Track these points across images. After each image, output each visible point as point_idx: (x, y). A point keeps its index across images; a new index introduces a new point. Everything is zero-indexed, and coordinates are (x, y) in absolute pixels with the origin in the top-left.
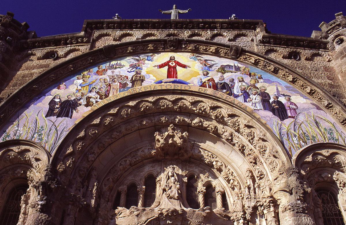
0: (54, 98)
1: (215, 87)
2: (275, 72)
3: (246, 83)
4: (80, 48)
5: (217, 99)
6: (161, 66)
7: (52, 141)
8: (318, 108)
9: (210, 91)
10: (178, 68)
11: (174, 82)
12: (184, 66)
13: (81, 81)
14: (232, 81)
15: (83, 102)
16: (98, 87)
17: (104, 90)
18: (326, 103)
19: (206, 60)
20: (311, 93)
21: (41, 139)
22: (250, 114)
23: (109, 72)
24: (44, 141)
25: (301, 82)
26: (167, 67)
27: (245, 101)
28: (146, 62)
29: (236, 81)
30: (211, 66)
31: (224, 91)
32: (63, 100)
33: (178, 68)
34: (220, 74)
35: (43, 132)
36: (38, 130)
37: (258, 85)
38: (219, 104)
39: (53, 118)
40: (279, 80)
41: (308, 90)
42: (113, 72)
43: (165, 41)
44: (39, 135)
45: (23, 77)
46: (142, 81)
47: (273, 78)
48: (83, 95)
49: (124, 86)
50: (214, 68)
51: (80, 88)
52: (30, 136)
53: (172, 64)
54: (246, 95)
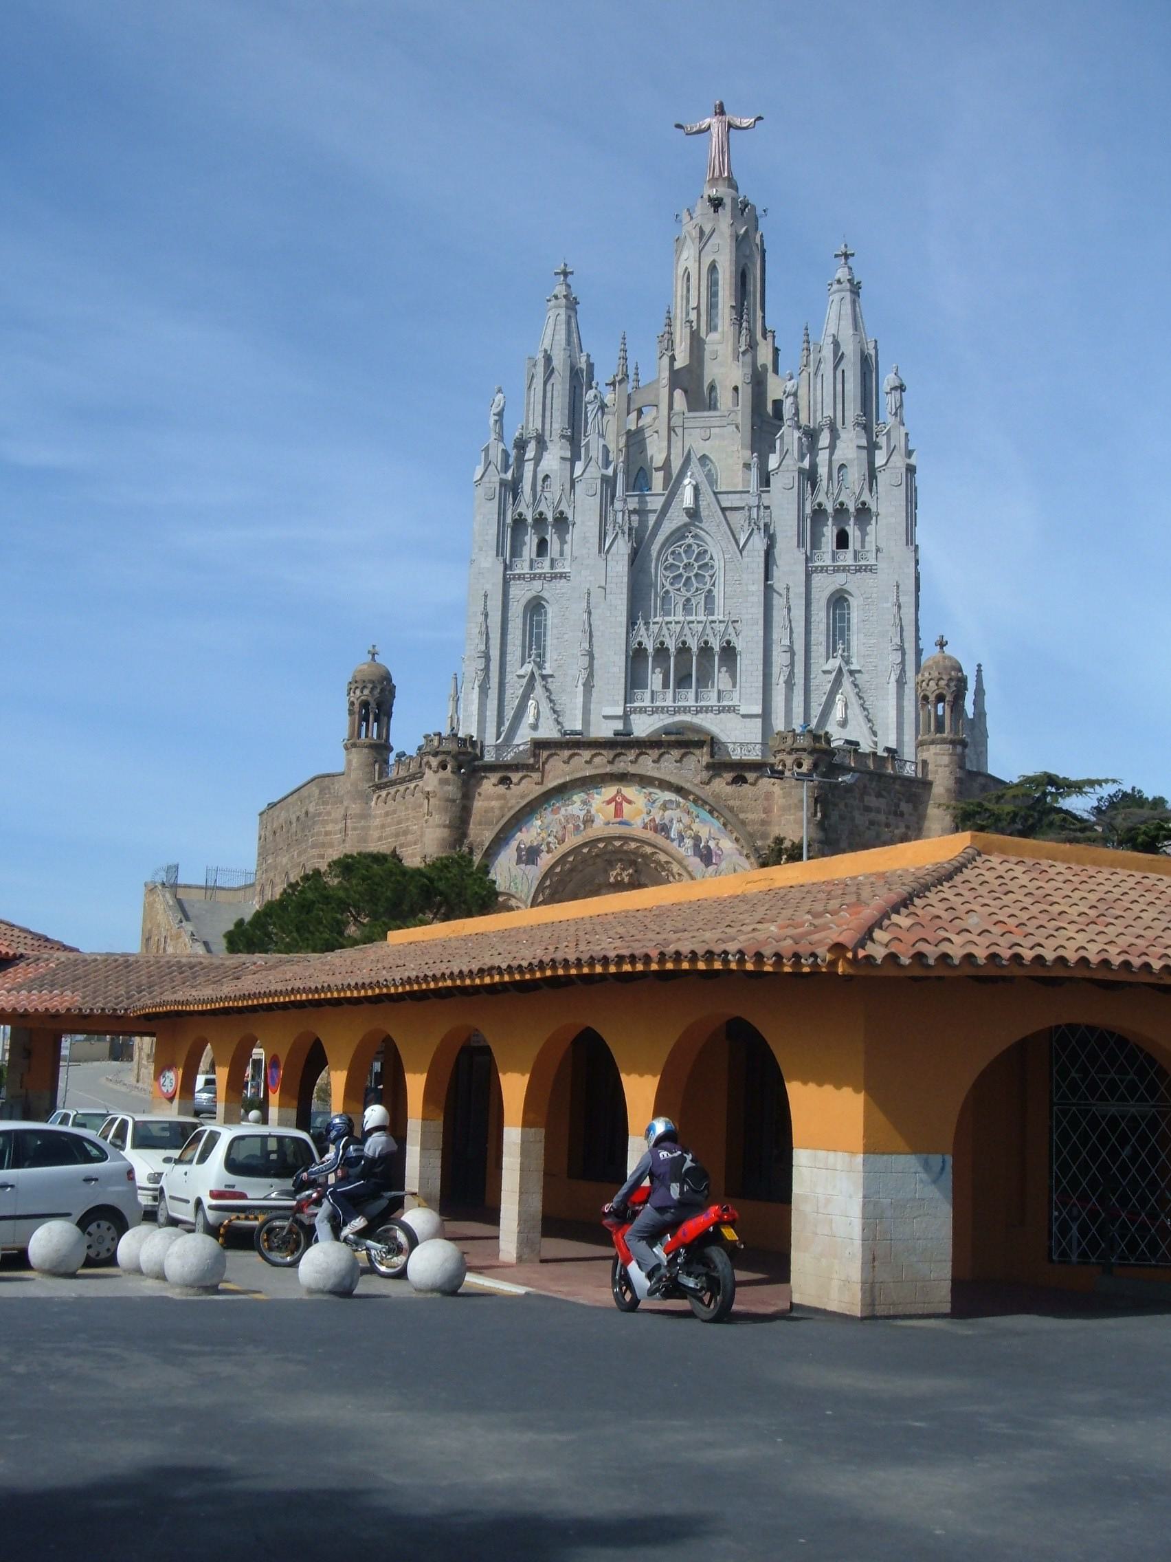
0: (519, 844)
1: (656, 831)
2: (711, 812)
3: (684, 824)
4: (532, 774)
5: (655, 846)
6: (609, 802)
7: (526, 890)
8: (741, 854)
9: (649, 835)
10: (625, 804)
11: (621, 823)
12: (630, 802)
13: (538, 823)
14: (671, 821)
15: (544, 847)
16: (555, 830)
17: (560, 834)
18: (745, 853)
19: (650, 793)
20: (737, 840)
21: (517, 888)
22: (680, 863)
23: (563, 811)
24: (520, 890)
25: (729, 827)
26: (614, 803)
27: (680, 846)
28: (596, 796)
29: (675, 822)
30: (654, 802)
31: (663, 834)
32: (527, 846)
33: (625, 804)
34: (661, 812)
35: (517, 881)
36: (513, 879)
37: (694, 827)
38: (657, 851)
39: (523, 866)
40: (714, 821)
41: (735, 835)
42: (566, 810)
43: (612, 774)
44: (515, 884)
45: (485, 812)
46: (593, 821)
47: (707, 816)
48: (543, 839)
49: (577, 828)
50: (656, 804)
51: (539, 830)
52: (508, 885)
53: (619, 799)
54: (681, 837)
